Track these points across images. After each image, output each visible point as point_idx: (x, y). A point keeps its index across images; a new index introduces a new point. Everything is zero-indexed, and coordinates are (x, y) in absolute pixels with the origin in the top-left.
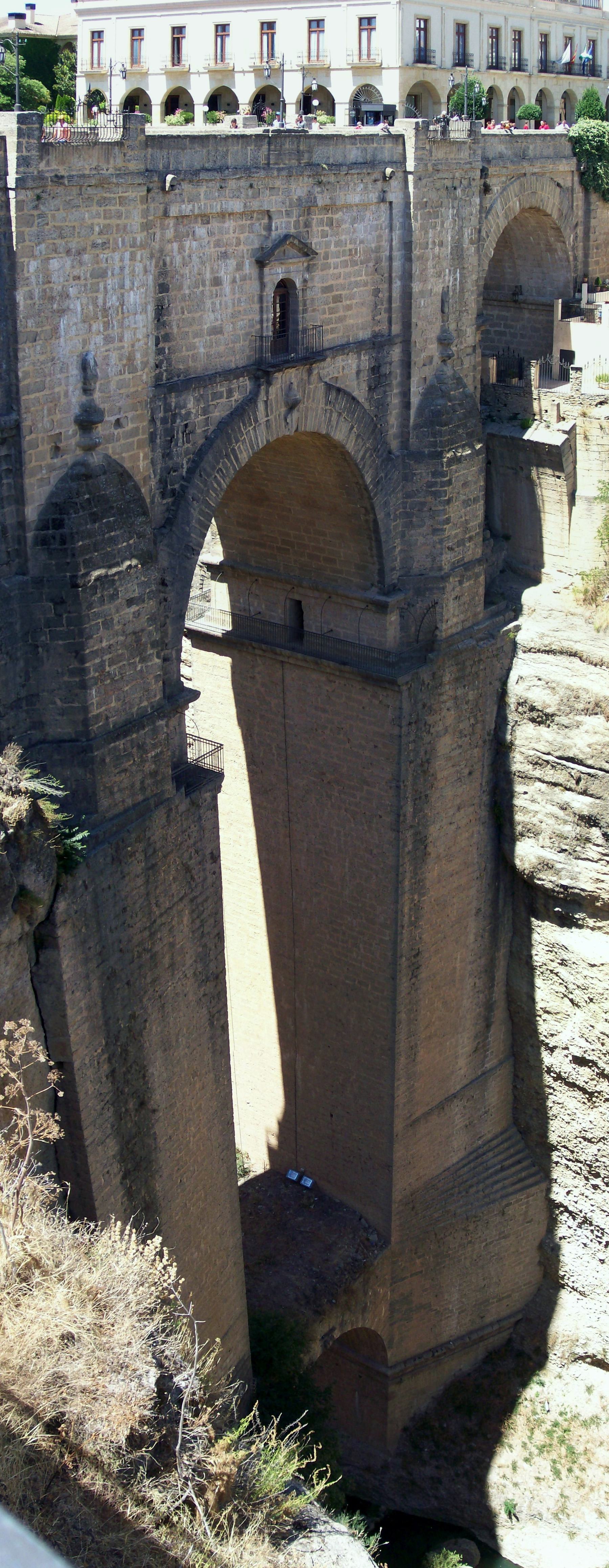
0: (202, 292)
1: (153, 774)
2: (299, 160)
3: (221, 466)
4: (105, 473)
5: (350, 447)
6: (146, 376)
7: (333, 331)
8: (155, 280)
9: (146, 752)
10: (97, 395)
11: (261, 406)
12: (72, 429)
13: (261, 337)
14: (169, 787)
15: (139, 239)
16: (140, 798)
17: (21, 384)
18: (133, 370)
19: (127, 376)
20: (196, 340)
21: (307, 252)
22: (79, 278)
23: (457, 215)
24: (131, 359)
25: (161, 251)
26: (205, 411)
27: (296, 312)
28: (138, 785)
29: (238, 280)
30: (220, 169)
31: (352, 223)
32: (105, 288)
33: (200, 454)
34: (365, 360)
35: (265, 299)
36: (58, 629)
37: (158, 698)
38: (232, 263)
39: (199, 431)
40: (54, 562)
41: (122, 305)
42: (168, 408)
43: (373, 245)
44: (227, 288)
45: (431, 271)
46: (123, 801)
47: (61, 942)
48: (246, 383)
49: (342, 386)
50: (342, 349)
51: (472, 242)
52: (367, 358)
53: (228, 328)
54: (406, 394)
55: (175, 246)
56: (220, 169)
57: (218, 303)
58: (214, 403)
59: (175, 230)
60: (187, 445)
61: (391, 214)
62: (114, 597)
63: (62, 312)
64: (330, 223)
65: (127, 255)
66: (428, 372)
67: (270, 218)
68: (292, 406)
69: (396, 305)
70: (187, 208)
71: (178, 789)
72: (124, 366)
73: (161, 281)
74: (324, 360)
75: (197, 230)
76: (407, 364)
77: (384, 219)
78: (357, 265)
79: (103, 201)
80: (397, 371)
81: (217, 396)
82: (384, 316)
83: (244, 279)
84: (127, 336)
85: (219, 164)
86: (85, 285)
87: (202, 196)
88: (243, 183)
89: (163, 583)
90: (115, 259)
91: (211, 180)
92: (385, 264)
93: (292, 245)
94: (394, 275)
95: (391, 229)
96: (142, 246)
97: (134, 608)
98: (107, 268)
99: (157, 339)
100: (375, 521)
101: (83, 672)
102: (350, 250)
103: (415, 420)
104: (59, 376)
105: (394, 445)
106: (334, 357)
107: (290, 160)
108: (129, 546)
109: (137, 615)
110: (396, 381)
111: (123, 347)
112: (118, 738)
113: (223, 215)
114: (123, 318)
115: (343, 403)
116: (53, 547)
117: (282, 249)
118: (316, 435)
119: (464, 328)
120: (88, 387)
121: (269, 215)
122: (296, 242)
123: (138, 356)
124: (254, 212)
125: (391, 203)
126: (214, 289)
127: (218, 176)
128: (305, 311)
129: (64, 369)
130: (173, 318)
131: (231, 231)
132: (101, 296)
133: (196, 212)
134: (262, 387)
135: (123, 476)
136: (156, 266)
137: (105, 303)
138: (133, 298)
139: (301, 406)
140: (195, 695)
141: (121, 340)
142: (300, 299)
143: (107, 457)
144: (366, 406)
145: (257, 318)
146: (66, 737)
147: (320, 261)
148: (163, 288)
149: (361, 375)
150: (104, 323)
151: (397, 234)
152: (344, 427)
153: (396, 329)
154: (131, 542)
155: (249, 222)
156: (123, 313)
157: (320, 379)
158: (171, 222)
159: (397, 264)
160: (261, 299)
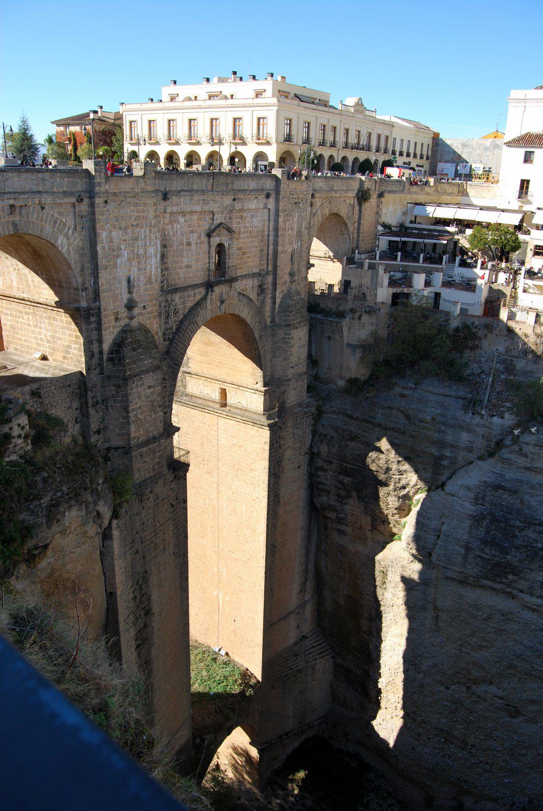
0: (182, 249)
2: (227, 187)
3: (190, 328)
4: (138, 330)
5: (249, 321)
6: (157, 286)
7: (241, 268)
8: (160, 242)
9: (155, 454)
10: (134, 295)
11: (209, 301)
12: (124, 309)
13: (209, 270)
14: (165, 469)
15: (153, 223)
16: (152, 474)
17: (100, 289)
18: (152, 283)
19: (148, 286)
20: (180, 270)
21: (230, 230)
22: (126, 240)
23: (300, 216)
24: (150, 278)
25: (163, 229)
26: (184, 303)
27: (225, 259)
28: (151, 468)
29: (199, 243)
30: (190, 191)
31: (251, 218)
32: (138, 245)
33: (181, 322)
34: (256, 282)
35: (211, 252)
36: (117, 399)
37: (161, 429)
39: (181, 312)
40: (115, 369)
41: (146, 253)
42: (167, 301)
43: (261, 229)
44: (193, 246)
45: (287, 242)
46: (145, 475)
47: (114, 537)
48: (202, 291)
49: (245, 293)
50: (244, 277)
51: (306, 228)
52: (257, 280)
53: (194, 265)
54: (274, 298)
55: (170, 226)
56: (190, 191)
57: (189, 253)
58: (188, 299)
59: (170, 219)
60: (175, 318)
61: (269, 214)
62: (142, 385)
63: (118, 256)
65: (148, 231)
66: (285, 288)
67: (213, 214)
68: (222, 302)
69: (270, 257)
70: (175, 209)
71: (169, 470)
72: (147, 281)
73: (163, 243)
74: (237, 281)
75: (180, 220)
76: (275, 284)
77: (266, 217)
78: (253, 238)
79: (136, 204)
80: (270, 287)
81: (189, 296)
82: (265, 262)
83: (201, 243)
84: (148, 266)
85: (189, 188)
86: (129, 244)
87: (182, 204)
88: (201, 197)
89: (164, 379)
90: (143, 232)
91: (186, 196)
92: (266, 238)
93: (223, 227)
94: (270, 243)
96: (154, 227)
97: (151, 390)
98: (138, 236)
99: (162, 270)
100: (259, 354)
101: (128, 417)
102: (250, 231)
103: (278, 309)
104: (117, 286)
105: (268, 320)
106: (242, 280)
107: (222, 187)
108: (149, 362)
109: (152, 393)
110: (269, 292)
111: (146, 273)
112: (143, 447)
113: (192, 212)
114: (146, 260)
115: (245, 301)
116: (115, 362)
117: (219, 229)
118: (234, 315)
119: (301, 268)
120: (131, 291)
122: (225, 226)
123: (153, 277)
124: (206, 211)
125: (269, 209)
126: (188, 247)
127: (189, 193)
128: (229, 258)
129: (120, 282)
131: (195, 220)
132: (136, 249)
133: (179, 210)
134: (209, 293)
135: (145, 331)
136: (161, 236)
137: (138, 252)
138: (151, 250)
139: (227, 302)
140: (178, 429)
141: (145, 270)
142: (227, 253)
143: (139, 323)
144: (256, 303)
145: (208, 261)
146: (120, 446)
147: (236, 236)
148: (164, 246)
149: (254, 288)
150: (138, 261)
151: (272, 224)
152: (246, 311)
153: (270, 268)
154: (150, 361)
155: (204, 216)
156: (146, 257)
157: (236, 290)
158: (168, 215)
159: (271, 238)
160: (209, 253)
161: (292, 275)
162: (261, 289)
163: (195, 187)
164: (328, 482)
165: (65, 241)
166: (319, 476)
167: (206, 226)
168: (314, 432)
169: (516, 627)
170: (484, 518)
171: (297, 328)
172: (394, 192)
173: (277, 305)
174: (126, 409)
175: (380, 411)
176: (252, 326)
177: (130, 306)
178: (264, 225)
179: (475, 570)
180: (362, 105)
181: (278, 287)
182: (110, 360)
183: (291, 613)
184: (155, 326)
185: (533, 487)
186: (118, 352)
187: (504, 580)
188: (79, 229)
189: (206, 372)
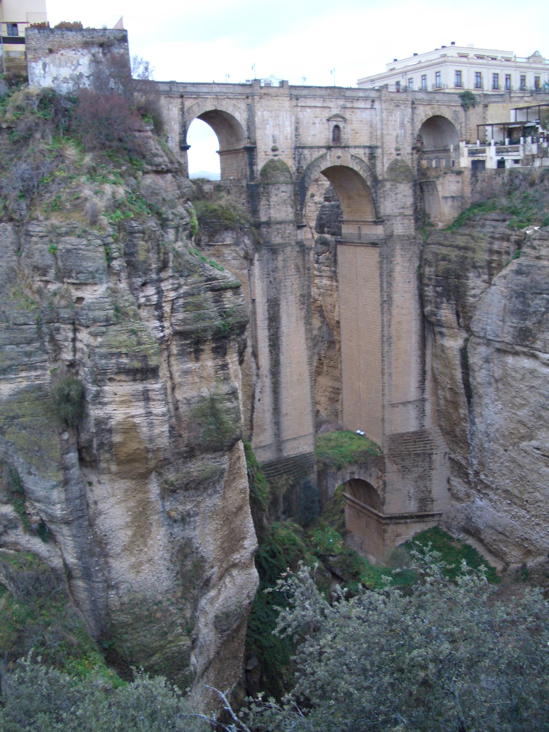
1: (289, 237)
5: (361, 173)
21: (344, 119)
25: (297, 115)
34: (367, 151)
38: (319, 119)
44: (317, 125)
53: (318, 136)
63: (267, 124)
69: (379, 137)
70: (304, 105)
76: (383, 154)
84: (285, 132)
121: (329, 107)
130: (301, 131)
135: (283, 164)
148: (297, 123)
151: (378, 118)
161: (397, 149)
162: (372, 157)
163: (317, 94)
164: (430, 294)
165: (239, 115)
166: (426, 291)
167: (326, 114)
168: (421, 259)
169: (539, 382)
171: (401, 183)
172: (498, 102)
175: (459, 237)
176: (364, 176)
177: (274, 150)
179: (510, 338)
181: (385, 155)
183: (410, 402)
184: (291, 163)
185: (539, 269)
187: (527, 343)
189: (351, 219)
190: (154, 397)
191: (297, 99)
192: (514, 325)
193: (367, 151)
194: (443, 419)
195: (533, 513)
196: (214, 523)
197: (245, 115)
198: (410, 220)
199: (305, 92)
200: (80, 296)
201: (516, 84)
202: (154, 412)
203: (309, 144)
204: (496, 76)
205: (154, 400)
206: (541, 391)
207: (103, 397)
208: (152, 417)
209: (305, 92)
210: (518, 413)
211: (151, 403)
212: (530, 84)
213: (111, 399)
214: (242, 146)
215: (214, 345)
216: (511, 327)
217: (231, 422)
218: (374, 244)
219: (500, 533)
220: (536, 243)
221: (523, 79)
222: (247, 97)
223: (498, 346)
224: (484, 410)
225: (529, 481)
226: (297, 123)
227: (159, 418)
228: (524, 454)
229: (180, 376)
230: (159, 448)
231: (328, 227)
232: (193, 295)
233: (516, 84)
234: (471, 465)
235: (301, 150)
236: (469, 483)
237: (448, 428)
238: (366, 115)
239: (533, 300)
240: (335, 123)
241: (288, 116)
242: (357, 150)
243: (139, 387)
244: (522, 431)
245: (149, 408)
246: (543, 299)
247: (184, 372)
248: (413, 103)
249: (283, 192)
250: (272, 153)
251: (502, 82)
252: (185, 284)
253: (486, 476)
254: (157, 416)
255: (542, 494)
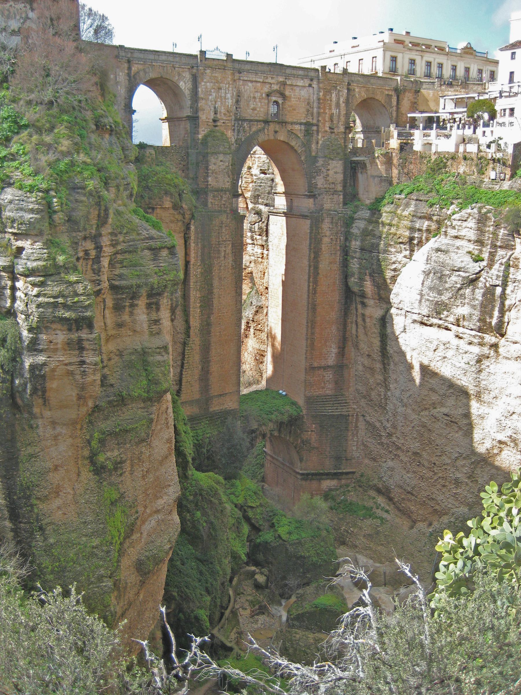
1: (224, 204)
10: (218, 116)
11: (266, 130)
21: (283, 95)
64: (292, 89)
70: (246, 78)
84: (227, 104)
95: (314, 94)
101: (207, 173)
112: (216, 191)
148: (239, 96)
162: (308, 133)
167: (266, 89)
170: (430, 273)
171: (333, 160)
173: (319, 145)
174: (207, 168)
178: (310, 96)
179: (426, 310)
180: (471, 48)
182: (202, 143)
186: (206, 140)
188: (191, 80)
190: (88, 347)
191: (240, 73)
192: (431, 299)
193: (303, 127)
194: (361, 384)
195: (440, 475)
196: (140, 469)
197: (190, 85)
198: (340, 195)
199: (248, 67)
200: (21, 245)
201: (447, 72)
202: (88, 361)
203: (249, 118)
204: (429, 64)
205: (88, 350)
206: (453, 362)
207: (39, 344)
208: (84, 366)
209: (248, 67)
210: (430, 381)
211: (85, 352)
212: (460, 72)
213: (46, 347)
214: (185, 115)
215: (148, 301)
216: (428, 300)
217: (160, 375)
218: (304, 217)
219: (408, 493)
220: (454, 223)
221: (454, 68)
222: (193, 67)
223: (416, 317)
224: (399, 377)
225: (437, 445)
226: (239, 96)
227: (92, 367)
228: (434, 420)
229: (114, 328)
230: (91, 395)
231: (262, 198)
232: (130, 252)
233: (447, 72)
234: (385, 428)
235: (240, 122)
236: (382, 444)
237: (365, 392)
238: (304, 93)
239: (450, 276)
240: (274, 99)
241: (230, 89)
242: (294, 126)
243: (74, 336)
244: (433, 398)
245: (82, 357)
246: (459, 276)
247: (119, 325)
248: (349, 84)
249: (221, 161)
250: (213, 124)
251: (435, 70)
252: (124, 242)
253: (399, 438)
254: (88, 364)
255: (450, 458)
